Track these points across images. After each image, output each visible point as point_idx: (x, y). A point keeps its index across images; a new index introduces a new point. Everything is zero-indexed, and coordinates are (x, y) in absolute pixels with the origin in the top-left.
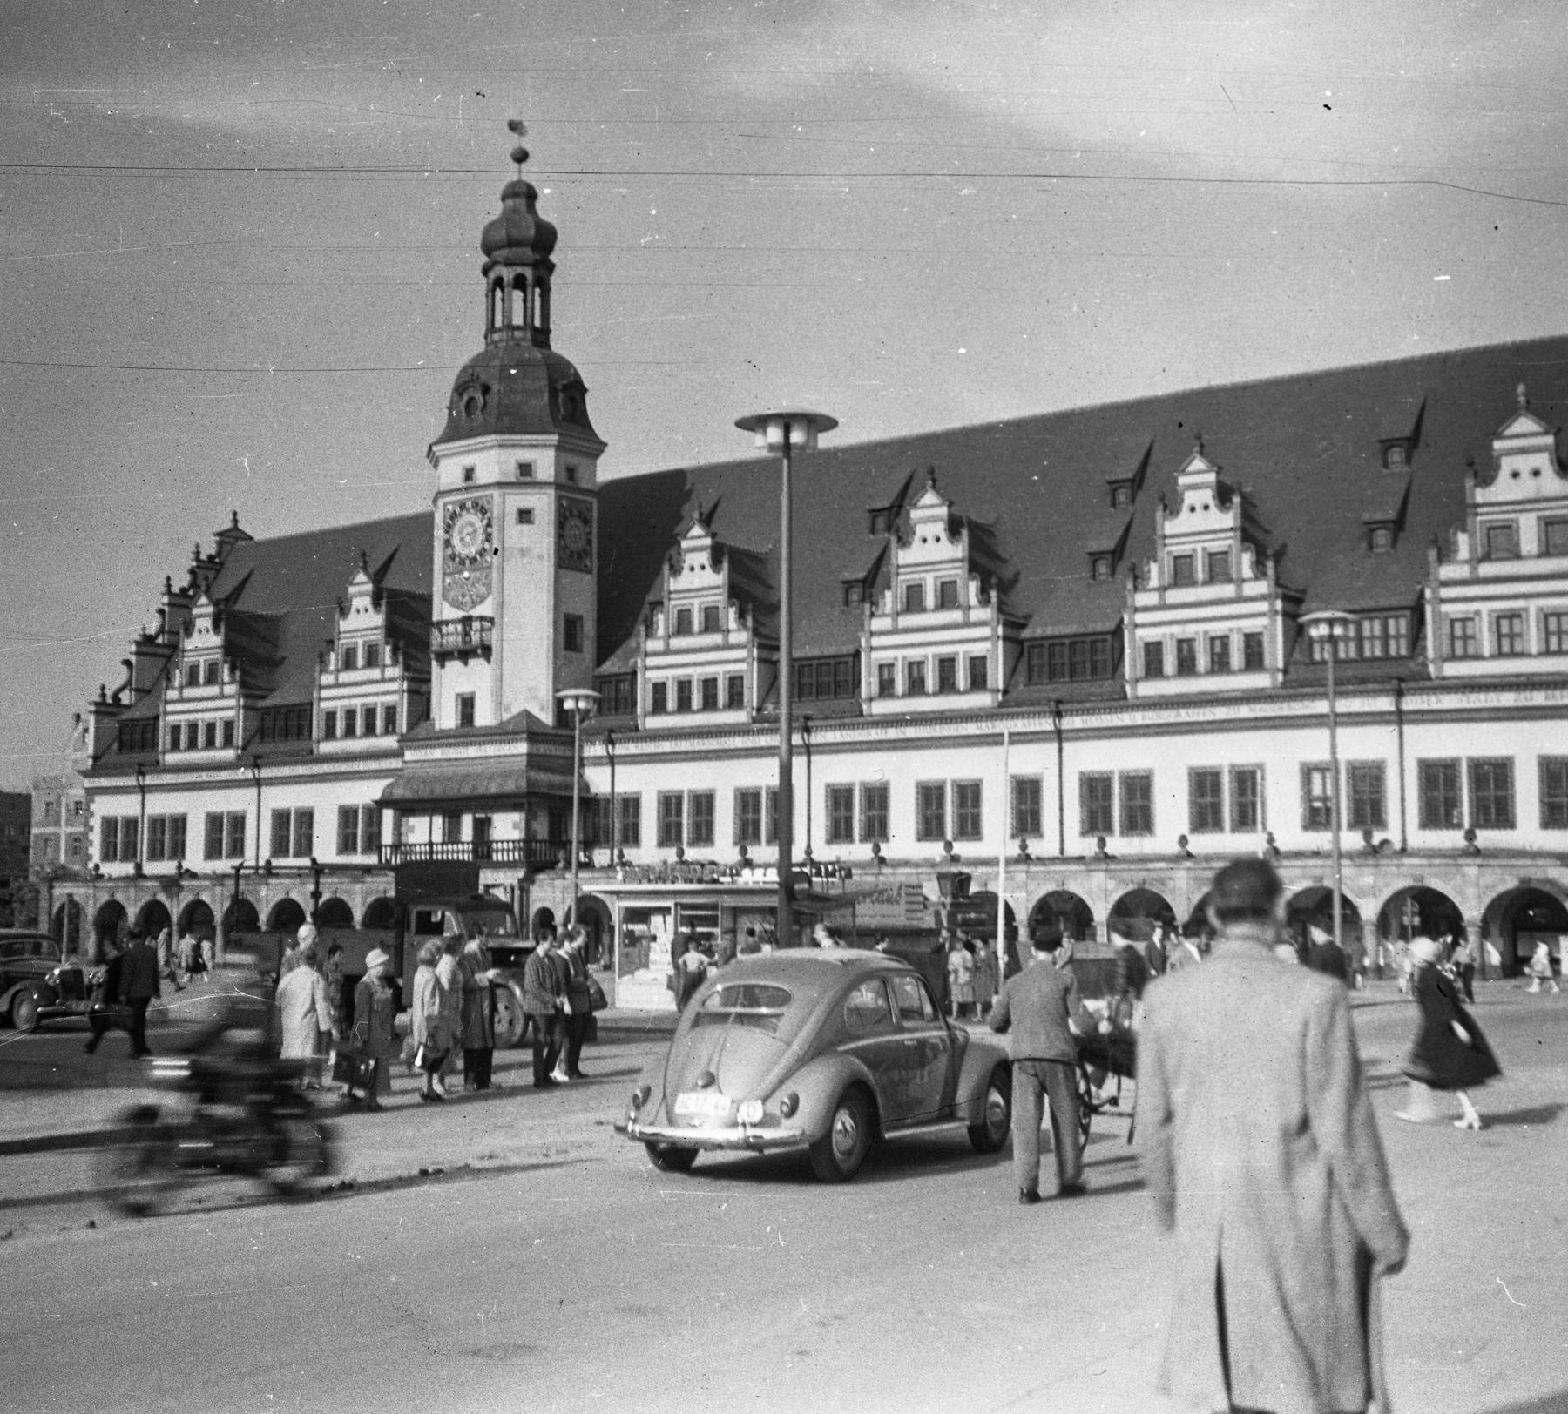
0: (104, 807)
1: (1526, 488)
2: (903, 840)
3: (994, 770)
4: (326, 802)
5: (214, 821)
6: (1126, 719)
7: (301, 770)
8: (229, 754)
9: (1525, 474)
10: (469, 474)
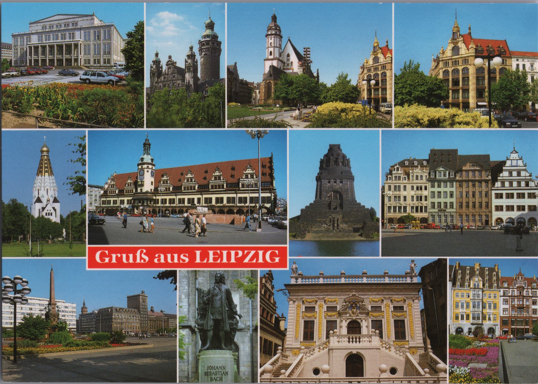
2: (186, 204)
3: (196, 197)
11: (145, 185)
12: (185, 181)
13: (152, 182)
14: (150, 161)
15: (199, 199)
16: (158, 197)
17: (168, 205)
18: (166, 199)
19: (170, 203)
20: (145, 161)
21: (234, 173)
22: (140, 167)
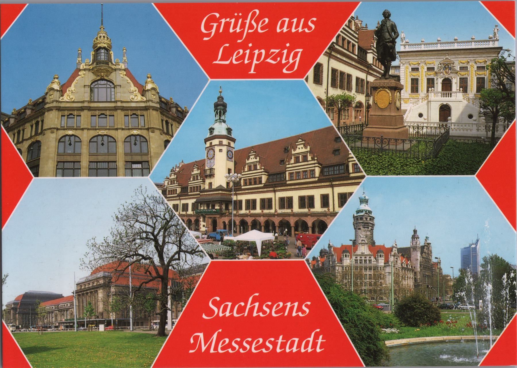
2: (296, 208)
3: (317, 194)
4: (190, 202)
6: (350, 182)
8: (176, 195)
10: (211, 143)
11: (215, 176)
12: (292, 161)
14: (224, 133)
15: (325, 200)
16: (240, 197)
17: (258, 211)
18: (254, 201)
19: (263, 207)
20: (216, 133)
22: (208, 144)
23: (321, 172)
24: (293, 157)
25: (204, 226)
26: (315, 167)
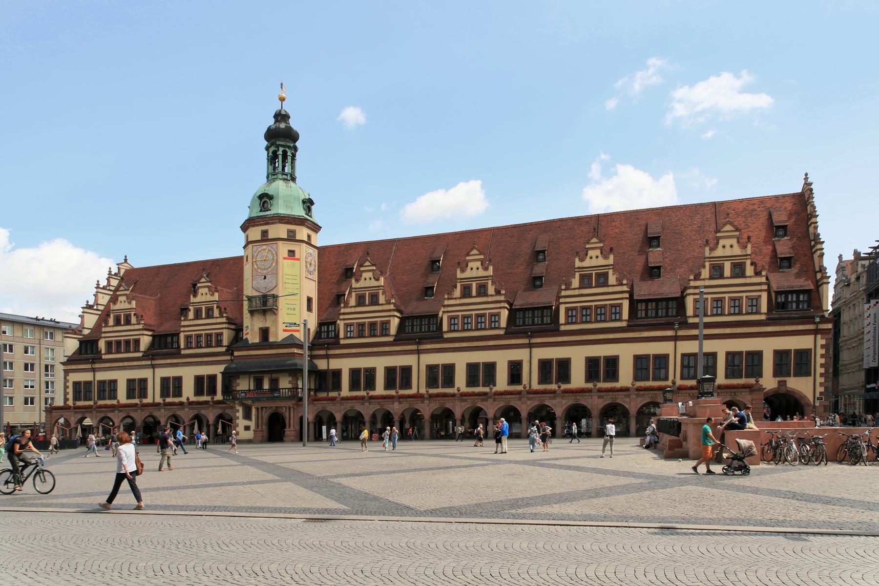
0: (74, 377)
1: (728, 252)
3: (502, 359)
4: (188, 375)
5: (130, 382)
7: (175, 361)
8: (140, 355)
9: (728, 247)
12: (457, 292)
13: (309, 300)
18: (371, 373)
21: (655, 255)
23: (511, 319)
24: (459, 285)
25: (247, 428)
26: (500, 308)
